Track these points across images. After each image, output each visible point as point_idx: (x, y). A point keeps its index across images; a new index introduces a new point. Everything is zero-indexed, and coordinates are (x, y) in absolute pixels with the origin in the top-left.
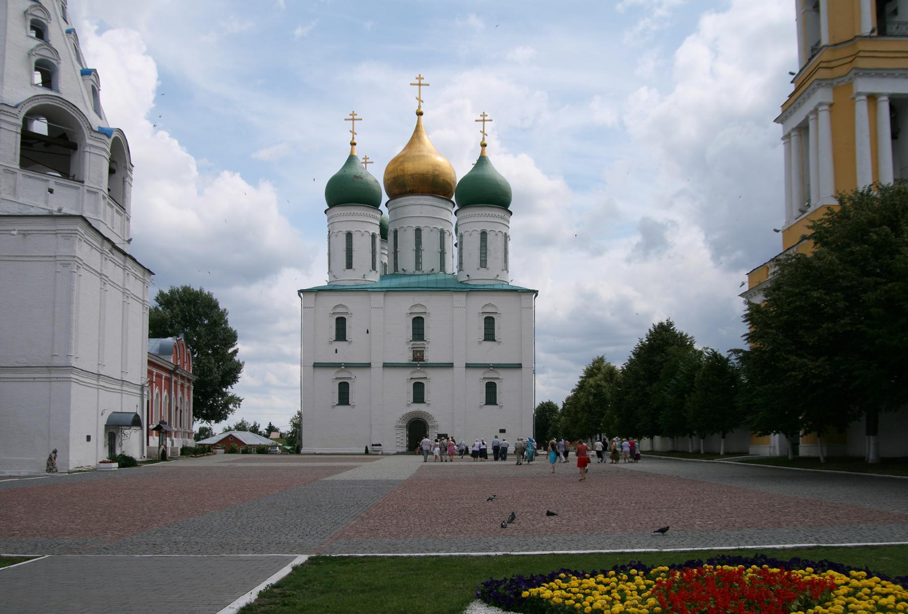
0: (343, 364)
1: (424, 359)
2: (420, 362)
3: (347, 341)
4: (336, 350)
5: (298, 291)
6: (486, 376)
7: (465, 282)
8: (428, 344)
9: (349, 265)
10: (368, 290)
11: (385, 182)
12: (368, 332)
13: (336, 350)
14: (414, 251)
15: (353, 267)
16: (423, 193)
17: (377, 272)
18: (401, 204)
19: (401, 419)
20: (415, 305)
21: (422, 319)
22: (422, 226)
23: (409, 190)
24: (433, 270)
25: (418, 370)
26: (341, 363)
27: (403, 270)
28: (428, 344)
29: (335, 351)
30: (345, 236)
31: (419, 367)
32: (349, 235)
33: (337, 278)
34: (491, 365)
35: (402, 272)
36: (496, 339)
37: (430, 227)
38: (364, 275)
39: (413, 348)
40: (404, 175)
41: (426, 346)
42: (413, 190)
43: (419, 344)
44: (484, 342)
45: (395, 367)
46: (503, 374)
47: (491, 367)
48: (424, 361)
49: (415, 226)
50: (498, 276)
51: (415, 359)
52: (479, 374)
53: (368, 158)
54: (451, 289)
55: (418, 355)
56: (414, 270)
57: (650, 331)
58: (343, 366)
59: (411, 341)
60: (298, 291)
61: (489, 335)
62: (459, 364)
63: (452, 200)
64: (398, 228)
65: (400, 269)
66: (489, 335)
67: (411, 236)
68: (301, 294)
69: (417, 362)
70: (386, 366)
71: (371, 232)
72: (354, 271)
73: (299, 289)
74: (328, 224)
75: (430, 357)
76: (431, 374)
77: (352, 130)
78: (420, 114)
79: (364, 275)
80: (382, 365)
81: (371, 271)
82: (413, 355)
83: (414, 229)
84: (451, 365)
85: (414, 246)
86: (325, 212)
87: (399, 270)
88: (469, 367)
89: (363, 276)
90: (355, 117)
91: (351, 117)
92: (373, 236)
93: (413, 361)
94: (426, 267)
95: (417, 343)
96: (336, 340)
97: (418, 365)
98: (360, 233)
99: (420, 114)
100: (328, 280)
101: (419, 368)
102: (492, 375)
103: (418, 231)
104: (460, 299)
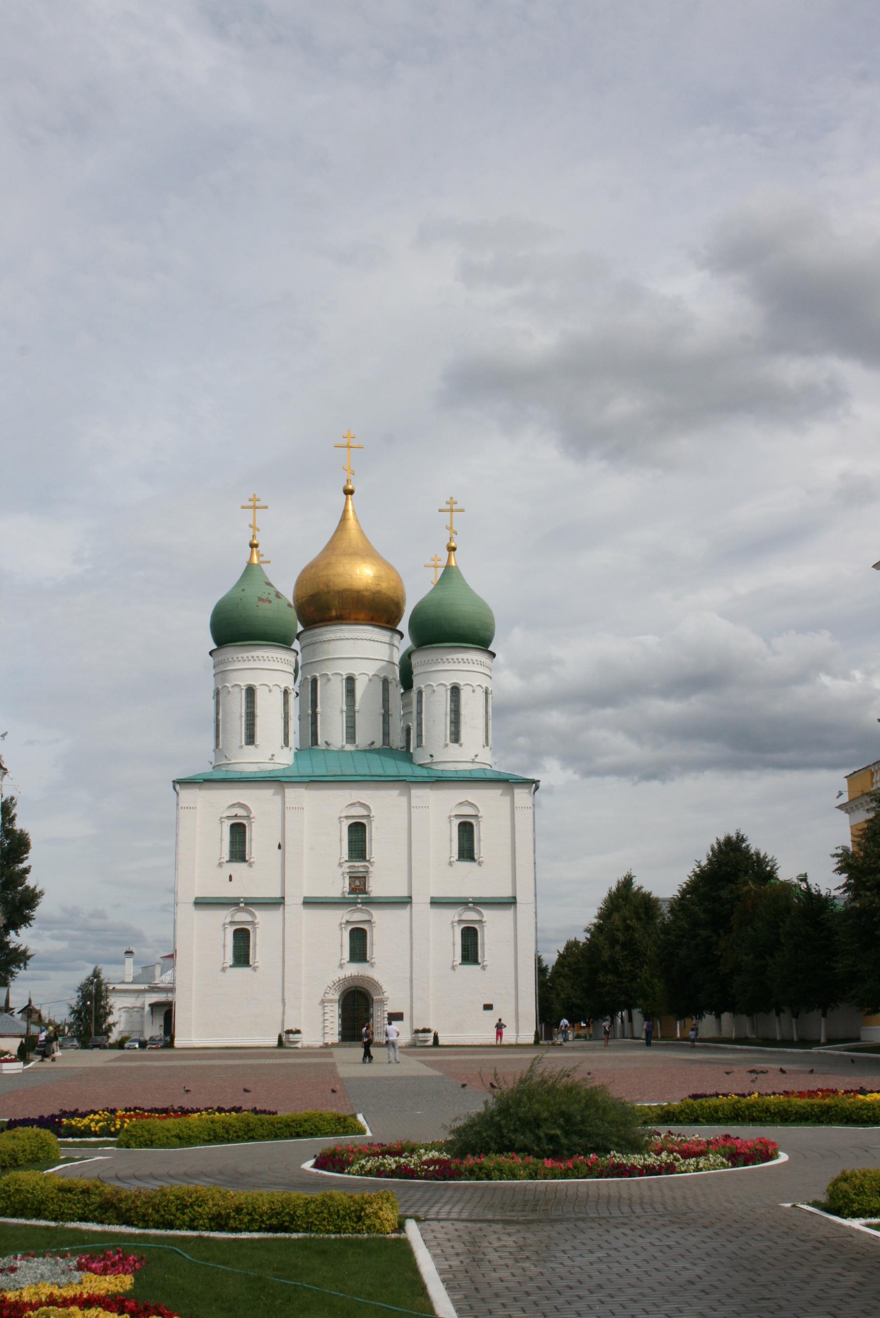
0: (242, 900)
1: (368, 889)
2: (360, 896)
3: (247, 861)
4: (231, 878)
5: (174, 782)
6: (464, 917)
7: (428, 766)
8: (372, 866)
9: (251, 739)
10: (283, 779)
11: (294, 603)
12: (280, 847)
13: (231, 878)
14: (344, 713)
15: (257, 743)
16: (357, 622)
17: (291, 749)
18: (324, 638)
19: (335, 984)
20: (353, 804)
21: (363, 826)
22: (356, 672)
23: (334, 613)
24: (373, 743)
25: (358, 908)
26: (239, 898)
27: (326, 743)
28: (372, 866)
29: (228, 878)
30: (244, 692)
31: (359, 903)
32: (251, 692)
33: (230, 760)
34: (470, 900)
35: (324, 747)
36: (476, 857)
37: (368, 675)
38: (273, 755)
39: (350, 872)
40: (329, 592)
41: (371, 869)
42: (342, 616)
43: (358, 867)
44: (460, 863)
45: (322, 903)
46: (489, 915)
47: (471, 902)
48: (366, 893)
49: (345, 673)
50: (476, 756)
51: (353, 891)
52: (453, 914)
53: (262, 556)
54: (408, 779)
55: (357, 883)
56: (344, 743)
57: (712, 850)
58: (242, 902)
59: (346, 861)
60: (174, 782)
61: (467, 852)
62: (421, 900)
63: (399, 628)
64: (317, 675)
65: (320, 741)
66: (467, 852)
67: (338, 689)
68: (178, 787)
69: (355, 896)
70: (309, 903)
71: (283, 686)
72: (257, 747)
73: (175, 779)
74: (213, 672)
75: (376, 888)
76: (378, 915)
77: (252, 523)
78: (348, 492)
79: (273, 755)
80: (302, 900)
81: (282, 748)
82: (350, 885)
83: (345, 677)
84: (409, 900)
85: (344, 705)
86: (211, 653)
87: (319, 742)
88: (435, 903)
89: (270, 757)
90: (258, 504)
91: (251, 504)
92: (286, 693)
93: (349, 893)
94: (363, 738)
95: (357, 864)
96: (230, 861)
97: (359, 901)
98: (267, 689)
99: (348, 492)
100: (213, 761)
101: (360, 906)
102: (471, 915)
103: (350, 681)
104: (420, 795)
